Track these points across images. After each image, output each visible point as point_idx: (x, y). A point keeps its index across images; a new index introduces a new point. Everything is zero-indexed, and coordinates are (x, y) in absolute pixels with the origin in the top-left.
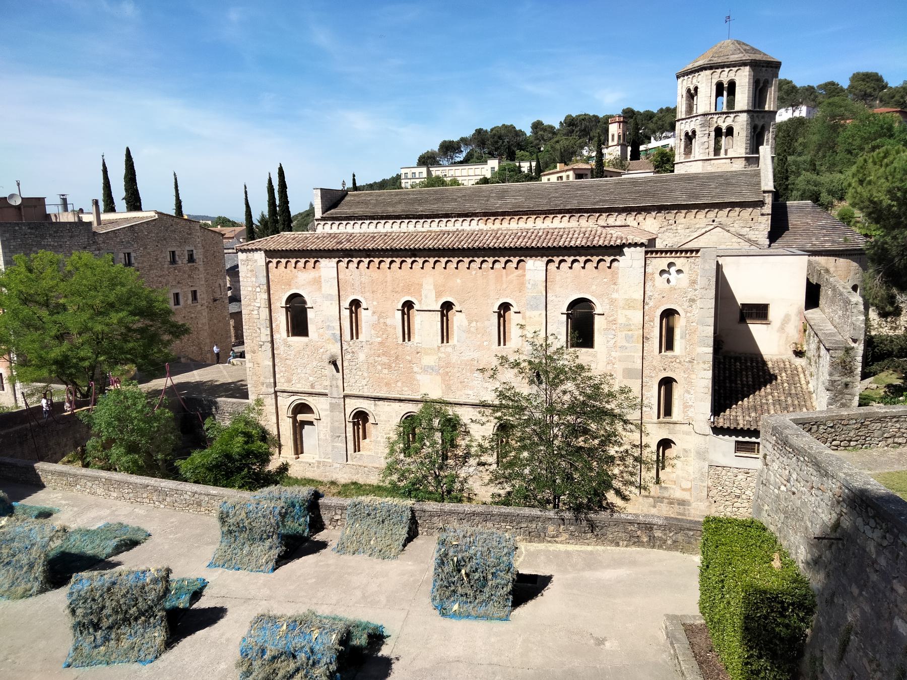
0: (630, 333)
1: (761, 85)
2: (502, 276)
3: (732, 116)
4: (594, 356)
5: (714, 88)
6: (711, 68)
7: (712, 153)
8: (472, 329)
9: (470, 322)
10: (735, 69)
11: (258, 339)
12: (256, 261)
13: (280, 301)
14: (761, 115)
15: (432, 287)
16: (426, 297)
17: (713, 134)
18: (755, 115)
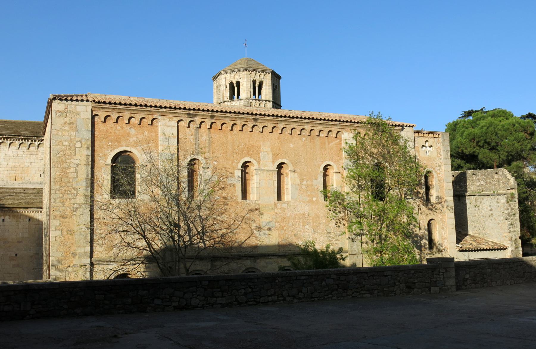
2: (325, 143)
3: (264, 103)
5: (252, 83)
6: (249, 71)
8: (303, 187)
9: (301, 182)
11: (73, 201)
12: (78, 114)
13: (104, 161)
15: (269, 150)
16: (264, 158)
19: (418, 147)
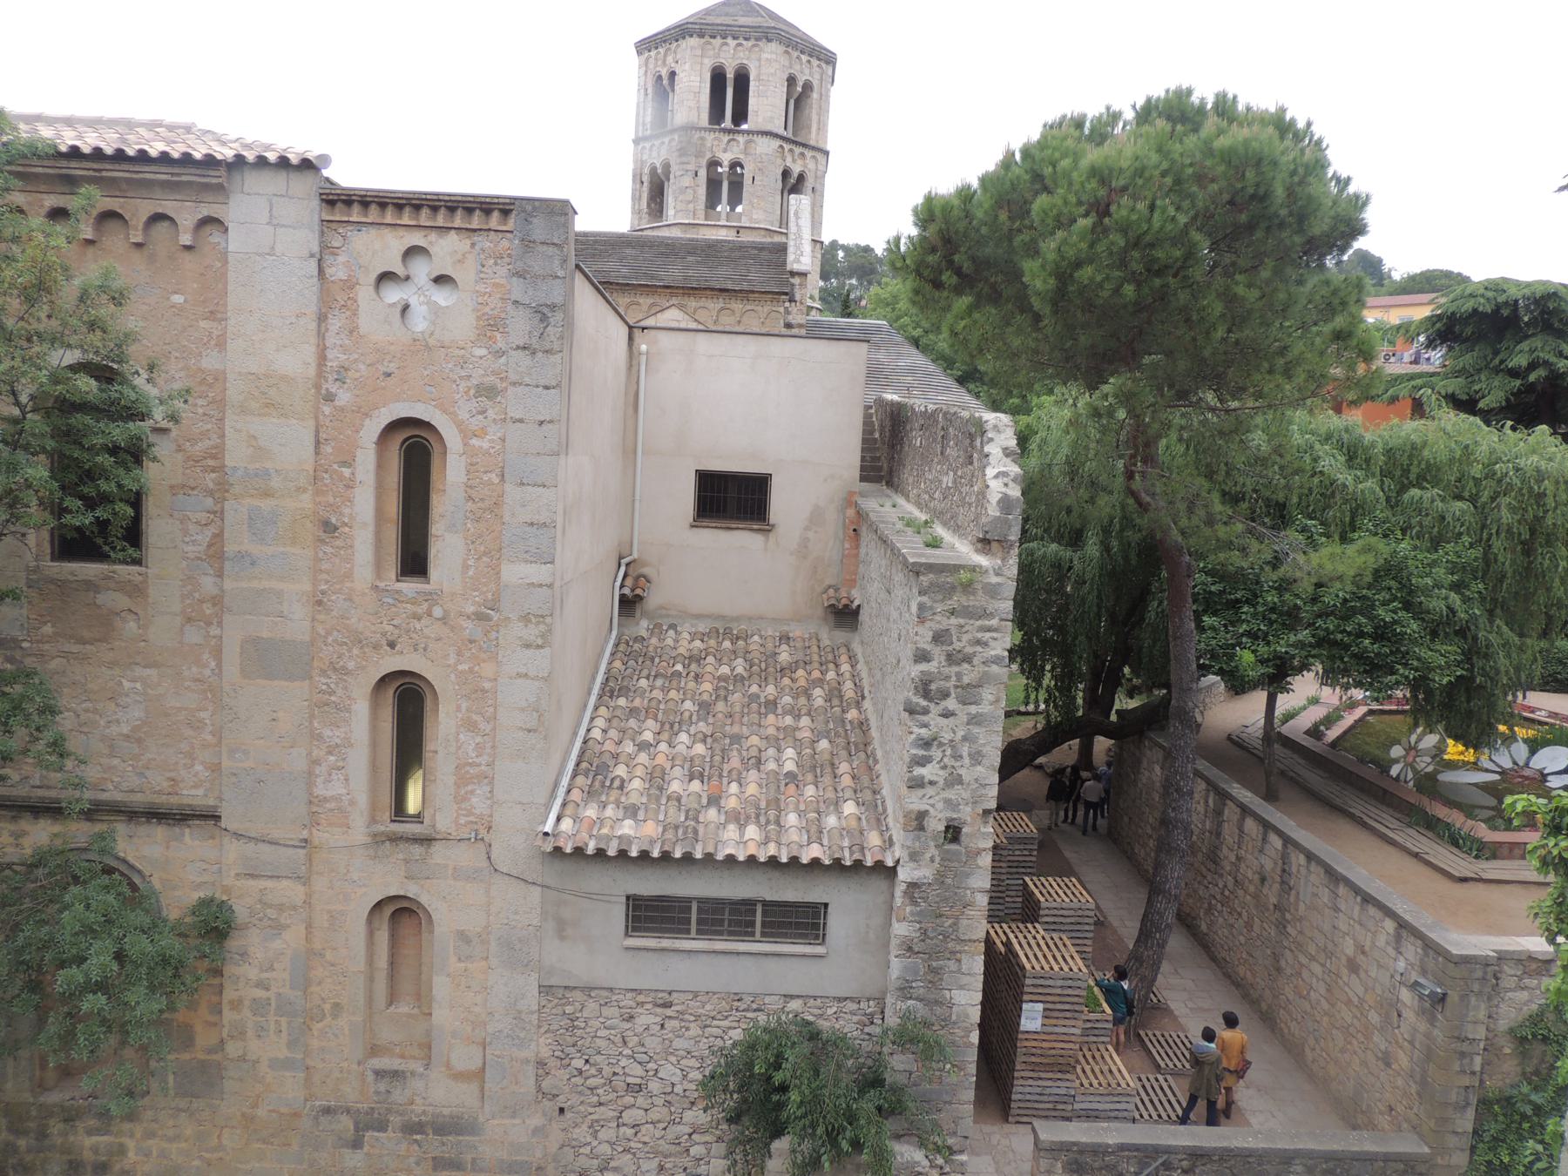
0: (266, 505)
1: (799, 89)
3: (741, 139)
4: (136, 591)
5: (708, 77)
6: (701, 36)
7: (701, 214)
14: (798, 150)
17: (703, 173)
18: (787, 147)
19: (350, 285)
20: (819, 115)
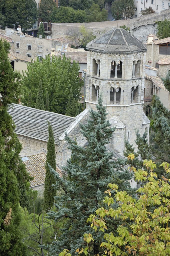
7: (91, 99)
10: (99, 54)
14: (115, 82)
17: (91, 88)
20: (124, 69)
